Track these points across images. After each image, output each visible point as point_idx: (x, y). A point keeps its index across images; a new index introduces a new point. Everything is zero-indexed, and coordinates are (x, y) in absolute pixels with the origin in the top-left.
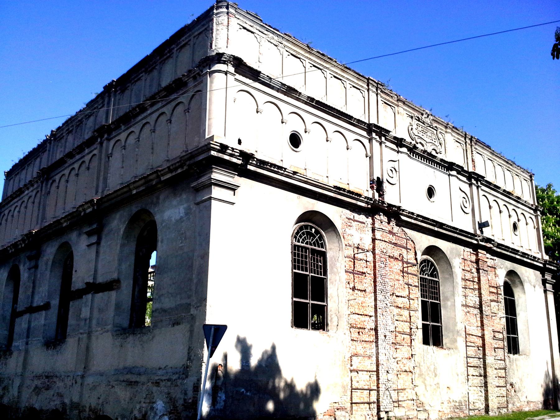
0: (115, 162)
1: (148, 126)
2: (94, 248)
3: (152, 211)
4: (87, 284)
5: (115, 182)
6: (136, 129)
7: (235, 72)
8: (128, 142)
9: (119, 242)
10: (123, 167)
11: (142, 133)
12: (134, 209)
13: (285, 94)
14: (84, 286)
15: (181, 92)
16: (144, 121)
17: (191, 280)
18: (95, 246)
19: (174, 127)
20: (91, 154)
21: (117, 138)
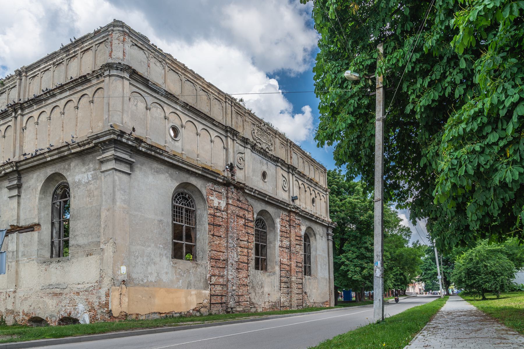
0: (30, 134)
1: (56, 109)
2: (15, 200)
3: (64, 175)
5: (30, 149)
6: (48, 109)
7: (130, 77)
8: (40, 119)
10: (37, 139)
11: (53, 114)
12: (49, 171)
13: (167, 98)
15: (85, 87)
16: (54, 105)
17: (100, 226)
19: (80, 113)
20: (6, 125)
21: (30, 115)
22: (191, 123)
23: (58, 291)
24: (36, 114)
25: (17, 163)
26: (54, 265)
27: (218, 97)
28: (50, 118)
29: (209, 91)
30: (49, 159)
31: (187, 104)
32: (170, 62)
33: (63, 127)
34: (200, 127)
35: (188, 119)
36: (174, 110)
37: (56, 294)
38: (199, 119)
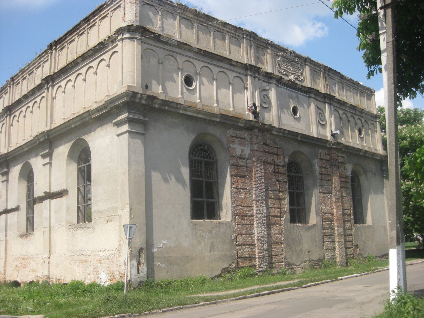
0: (58, 103)
4: (45, 192)
6: (72, 78)
9: (65, 162)
10: (64, 107)
14: (43, 194)
16: (78, 72)
18: (48, 165)
22: (207, 69)
23: (83, 258)
24: (63, 83)
25: (48, 132)
26: (79, 231)
27: (235, 35)
28: (74, 86)
29: (224, 30)
30: (73, 126)
31: (201, 50)
32: (181, 11)
33: (85, 93)
34: (216, 70)
35: (203, 64)
36: (187, 59)
37: (82, 262)
38: (215, 62)
